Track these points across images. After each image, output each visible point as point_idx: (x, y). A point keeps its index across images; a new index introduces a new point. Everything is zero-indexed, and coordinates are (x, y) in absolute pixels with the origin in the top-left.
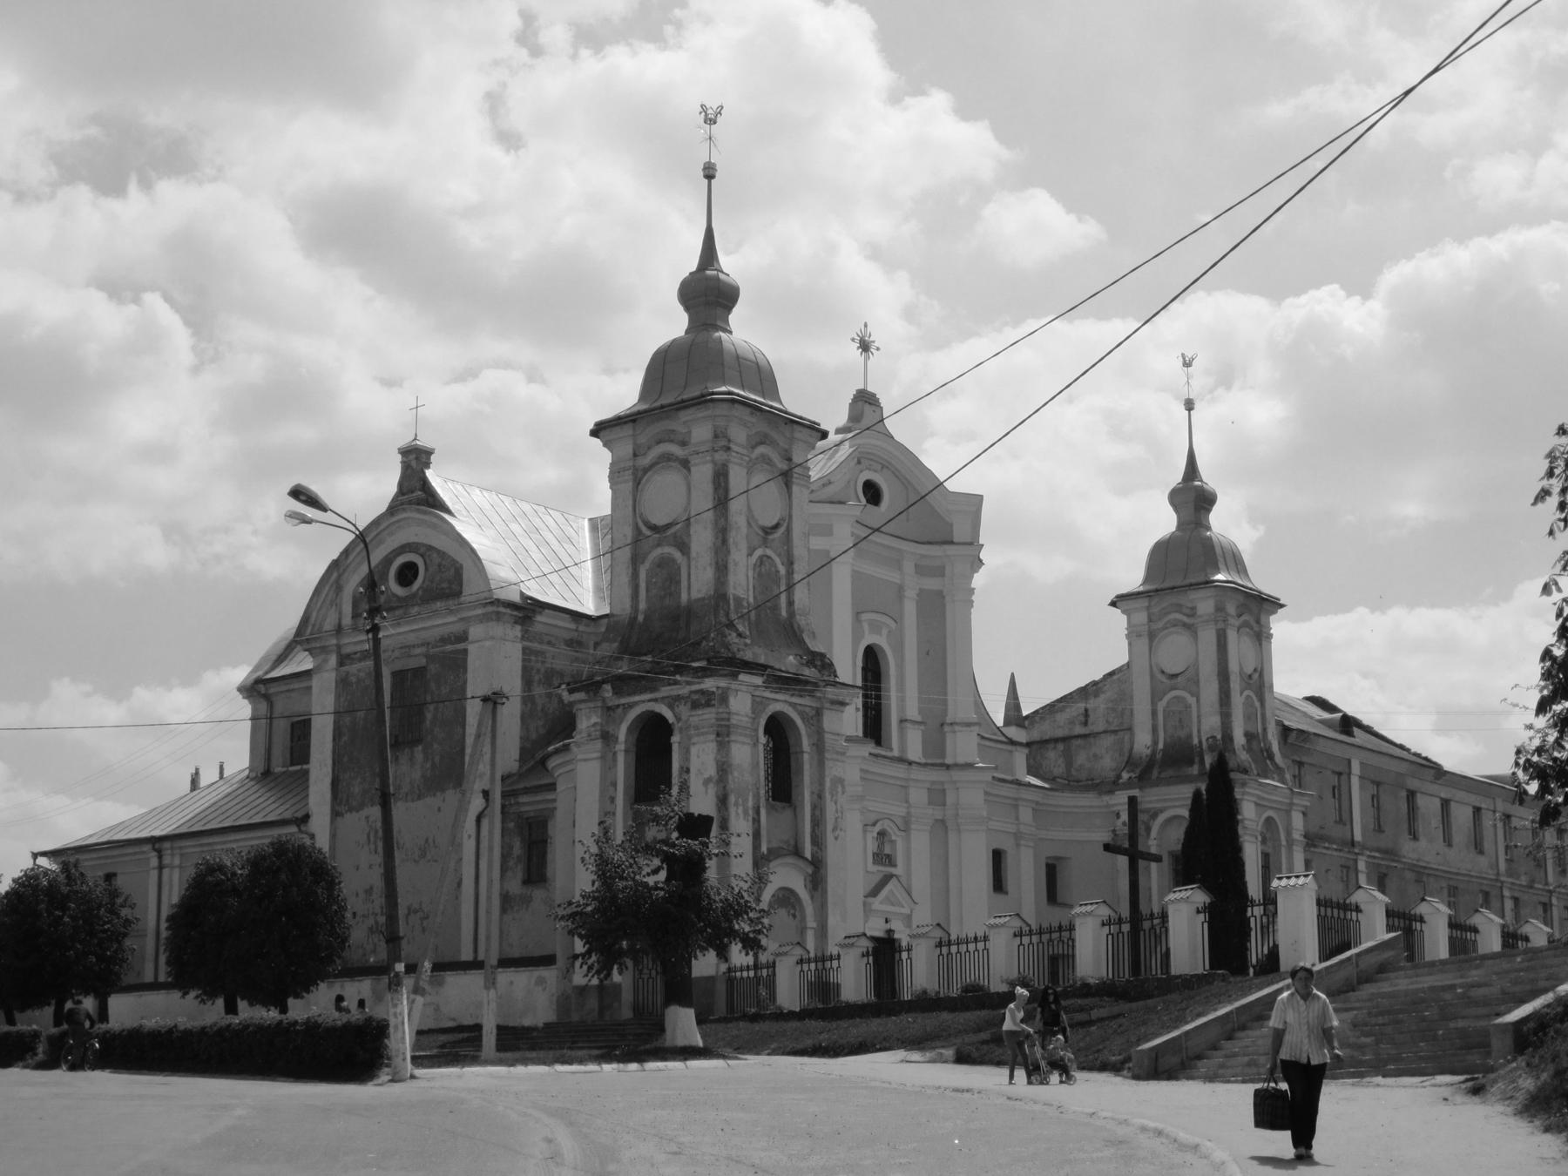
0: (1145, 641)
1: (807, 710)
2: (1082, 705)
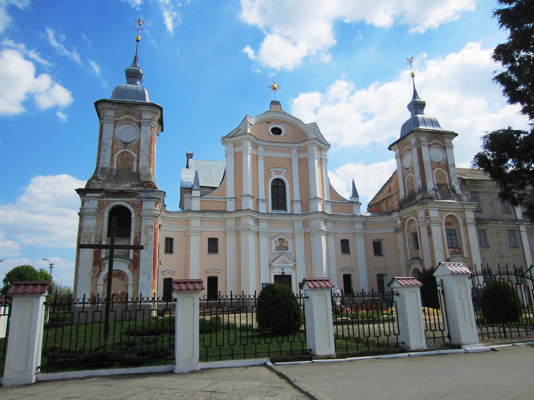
0: (399, 159)
1: (135, 202)
2: (389, 186)
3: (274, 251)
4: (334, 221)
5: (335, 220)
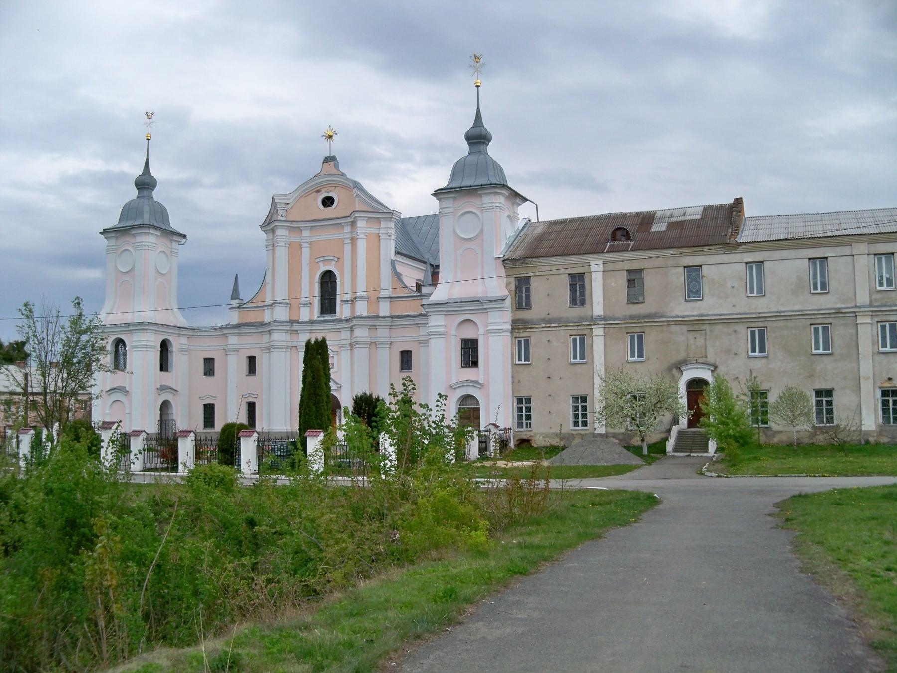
4: (391, 325)
5: (390, 324)
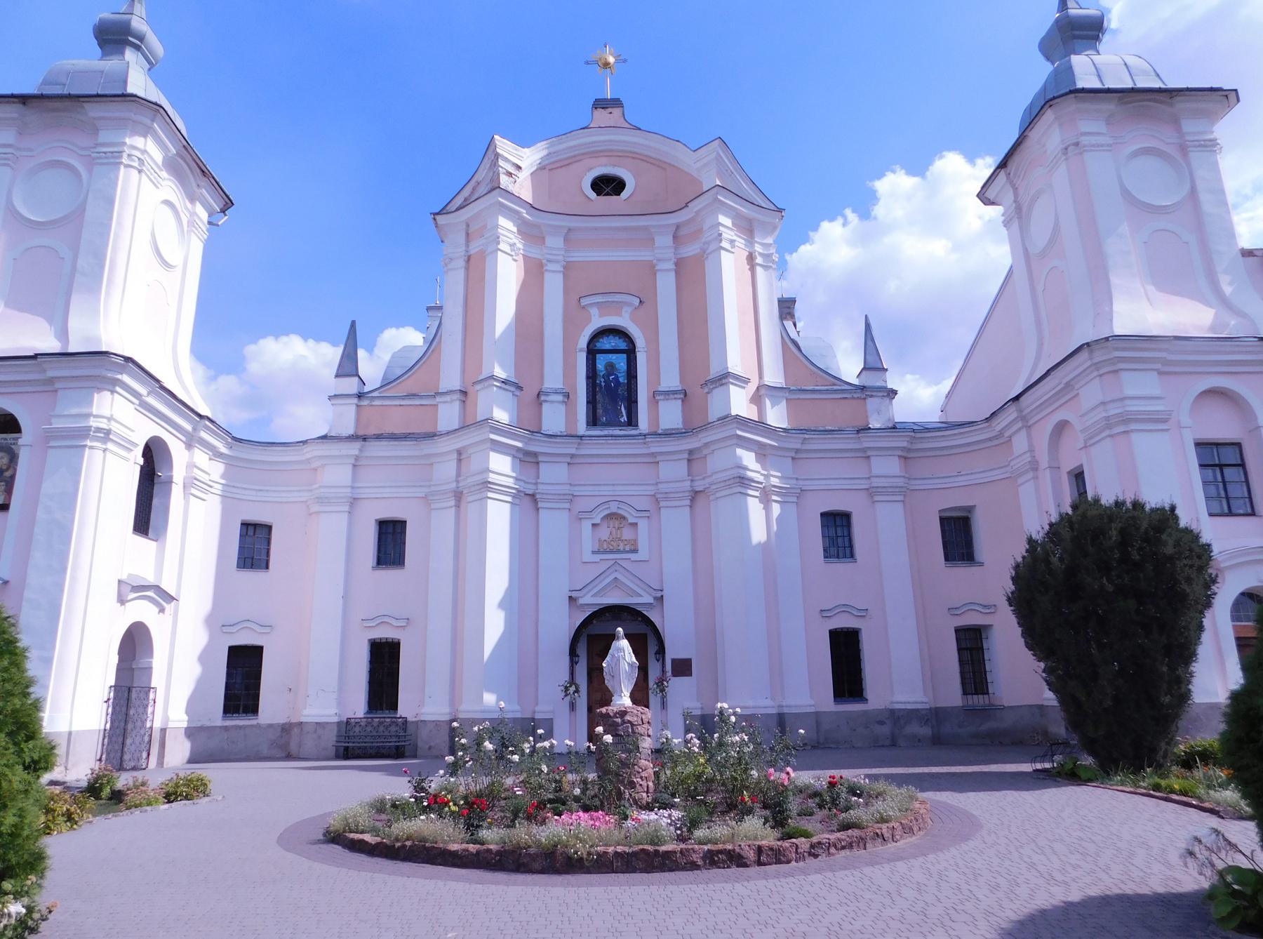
0: (1015, 225)
3: (588, 556)
5: (798, 446)
